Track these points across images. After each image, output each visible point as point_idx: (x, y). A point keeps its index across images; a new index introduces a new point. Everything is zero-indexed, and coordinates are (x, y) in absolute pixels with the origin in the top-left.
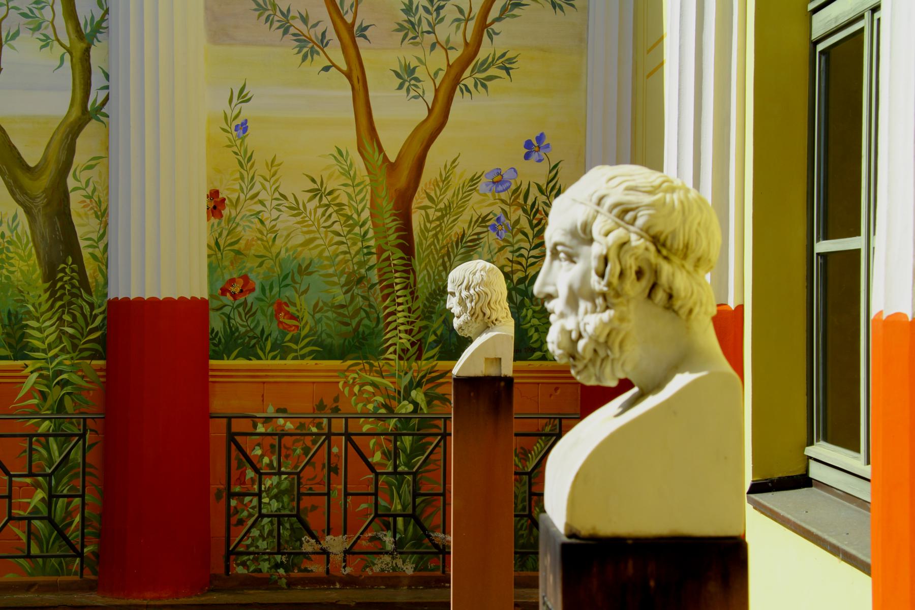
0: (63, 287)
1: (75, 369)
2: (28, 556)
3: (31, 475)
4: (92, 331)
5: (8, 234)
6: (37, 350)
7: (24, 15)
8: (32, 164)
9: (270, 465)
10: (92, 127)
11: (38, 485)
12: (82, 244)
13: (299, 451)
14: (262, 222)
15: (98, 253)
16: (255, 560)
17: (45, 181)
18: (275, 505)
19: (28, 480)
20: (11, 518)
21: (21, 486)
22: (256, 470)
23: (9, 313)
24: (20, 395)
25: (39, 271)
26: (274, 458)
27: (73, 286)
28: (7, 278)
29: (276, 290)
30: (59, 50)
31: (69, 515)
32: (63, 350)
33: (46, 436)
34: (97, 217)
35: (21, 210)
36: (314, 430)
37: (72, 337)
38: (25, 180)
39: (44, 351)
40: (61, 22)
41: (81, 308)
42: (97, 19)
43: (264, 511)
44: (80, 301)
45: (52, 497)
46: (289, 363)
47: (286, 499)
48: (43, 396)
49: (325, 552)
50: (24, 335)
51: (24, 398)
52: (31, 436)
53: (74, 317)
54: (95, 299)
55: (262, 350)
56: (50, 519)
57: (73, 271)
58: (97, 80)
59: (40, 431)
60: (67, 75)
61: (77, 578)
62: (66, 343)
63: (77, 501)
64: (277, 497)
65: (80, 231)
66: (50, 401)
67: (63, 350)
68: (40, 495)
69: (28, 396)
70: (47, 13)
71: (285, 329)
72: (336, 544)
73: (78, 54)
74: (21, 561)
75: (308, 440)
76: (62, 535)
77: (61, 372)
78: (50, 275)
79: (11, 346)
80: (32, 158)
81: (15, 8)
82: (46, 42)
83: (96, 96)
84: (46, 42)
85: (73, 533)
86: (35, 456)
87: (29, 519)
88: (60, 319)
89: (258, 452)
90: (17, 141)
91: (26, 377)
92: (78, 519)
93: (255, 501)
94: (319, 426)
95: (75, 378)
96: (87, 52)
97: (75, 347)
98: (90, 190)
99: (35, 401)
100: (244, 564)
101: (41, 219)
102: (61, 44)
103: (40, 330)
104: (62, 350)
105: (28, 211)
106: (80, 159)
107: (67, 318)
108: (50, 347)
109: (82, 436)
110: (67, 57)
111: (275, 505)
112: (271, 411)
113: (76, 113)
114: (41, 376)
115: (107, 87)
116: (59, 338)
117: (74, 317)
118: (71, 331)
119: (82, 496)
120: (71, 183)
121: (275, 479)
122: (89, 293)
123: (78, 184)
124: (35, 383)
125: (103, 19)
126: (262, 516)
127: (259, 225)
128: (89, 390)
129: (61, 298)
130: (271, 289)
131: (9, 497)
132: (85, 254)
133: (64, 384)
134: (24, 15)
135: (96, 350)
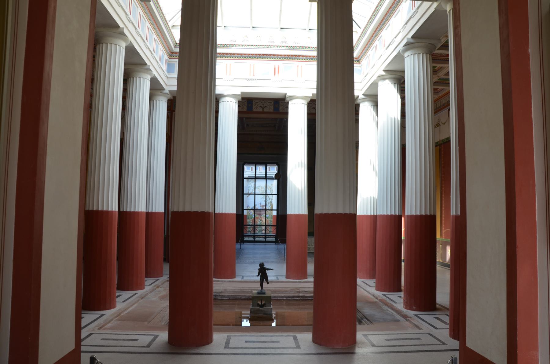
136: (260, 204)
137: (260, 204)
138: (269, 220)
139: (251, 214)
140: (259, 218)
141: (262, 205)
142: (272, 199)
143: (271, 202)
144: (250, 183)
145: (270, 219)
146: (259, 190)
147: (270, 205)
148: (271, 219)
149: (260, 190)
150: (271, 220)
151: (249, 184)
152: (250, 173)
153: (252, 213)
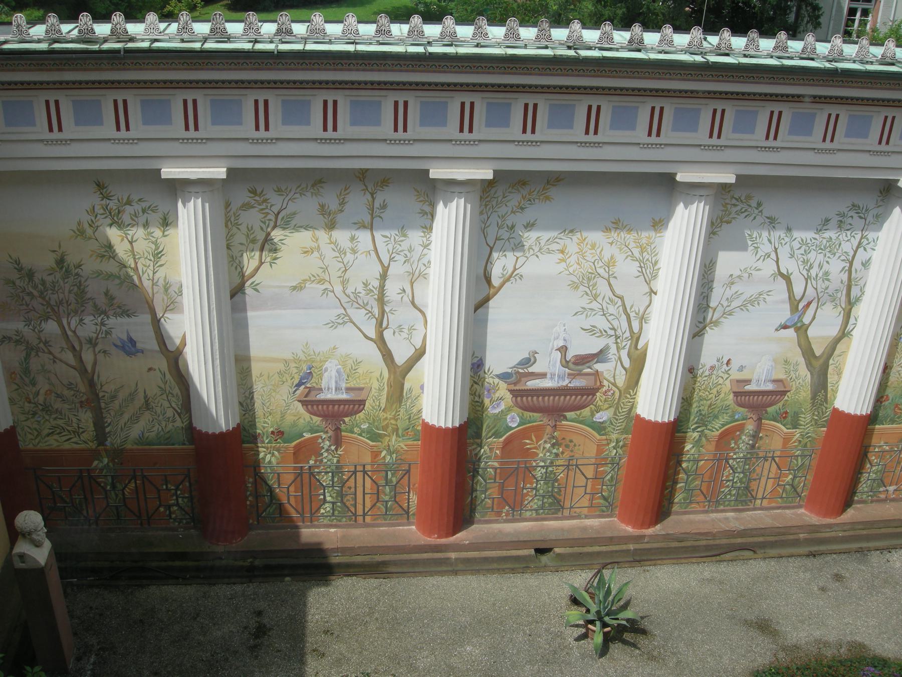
0: (817, 402)
1: (814, 432)
2: (781, 498)
3: (789, 470)
4: (826, 417)
5: (801, 382)
6: (801, 425)
7: (830, 296)
8: (817, 355)
9: (876, 463)
10: (846, 339)
11: (791, 474)
12: (829, 385)
13: (888, 457)
14: (899, 374)
15: (834, 388)
16: (862, 495)
17: (821, 361)
18: (874, 476)
19: (787, 472)
20: (778, 485)
21: (784, 474)
22: (871, 464)
23: (795, 412)
24: (793, 441)
25: (810, 396)
26: (879, 460)
27: (821, 401)
28: (797, 399)
29: (897, 400)
30: (840, 309)
31: (799, 483)
32: (811, 425)
33: (797, 456)
34: (838, 375)
35: (809, 373)
36: (896, 449)
37: (816, 420)
38: (814, 362)
39: (804, 426)
40: (843, 298)
41: (822, 409)
42: (858, 296)
43: (870, 478)
44: (823, 407)
45: (795, 477)
46: (894, 426)
47: (879, 474)
48: (800, 442)
49: (887, 491)
50: (798, 420)
51: (792, 443)
52: (792, 457)
53: (819, 413)
54: (828, 406)
55: (885, 421)
56: (792, 486)
57: (823, 395)
58: (852, 320)
59: (796, 454)
60: (840, 320)
61: (797, 504)
62: (813, 423)
63: (804, 478)
64: (876, 473)
65: (829, 380)
66: (802, 443)
67: (811, 425)
68: (791, 476)
69: (795, 442)
70: (839, 295)
71: (896, 413)
72: (891, 488)
73: (847, 311)
74: (779, 499)
75: (892, 453)
76: (795, 490)
77: (808, 433)
78: (814, 397)
79: (792, 424)
80: (818, 353)
81: (827, 293)
82: (835, 307)
83: (850, 327)
84: (835, 307)
85: (799, 490)
86: (792, 463)
87: (785, 485)
88: (813, 414)
89: (874, 458)
90: (814, 347)
91: (795, 435)
92: (802, 484)
93: (867, 475)
94: (898, 448)
95: (813, 435)
96: (851, 309)
97: (816, 423)
98: (837, 365)
99: (796, 444)
100: (857, 497)
101: (815, 376)
102: (841, 307)
103: (805, 418)
104: (811, 425)
105: (812, 374)
106: (837, 352)
107: (816, 413)
108: (807, 424)
109: (811, 456)
110: (843, 312)
111: (874, 476)
112: (882, 443)
113: (840, 334)
114: (801, 435)
115: (855, 324)
116: (811, 421)
117: (819, 413)
118: (816, 418)
119: (806, 477)
120: (831, 362)
121: (877, 467)
122: (827, 403)
123: (833, 362)
124: (799, 437)
125: (860, 296)
126: (868, 480)
127: (898, 376)
128: (817, 439)
129: (815, 406)
130: (896, 398)
131: (779, 478)
132: (829, 389)
133: (810, 437)
134: (830, 296)
135: (824, 425)
136: (563, 350)
137: (563, 350)
138: (609, 441)
139: (497, 411)
140: (549, 429)
141: (570, 355)
142: (643, 319)
143: (635, 338)
144: (503, 210)
145: (614, 436)
146: (562, 260)
147: (624, 354)
148: (624, 431)
149: (573, 260)
150: (618, 441)
151: (494, 219)
152: (511, 147)
153: (503, 407)
